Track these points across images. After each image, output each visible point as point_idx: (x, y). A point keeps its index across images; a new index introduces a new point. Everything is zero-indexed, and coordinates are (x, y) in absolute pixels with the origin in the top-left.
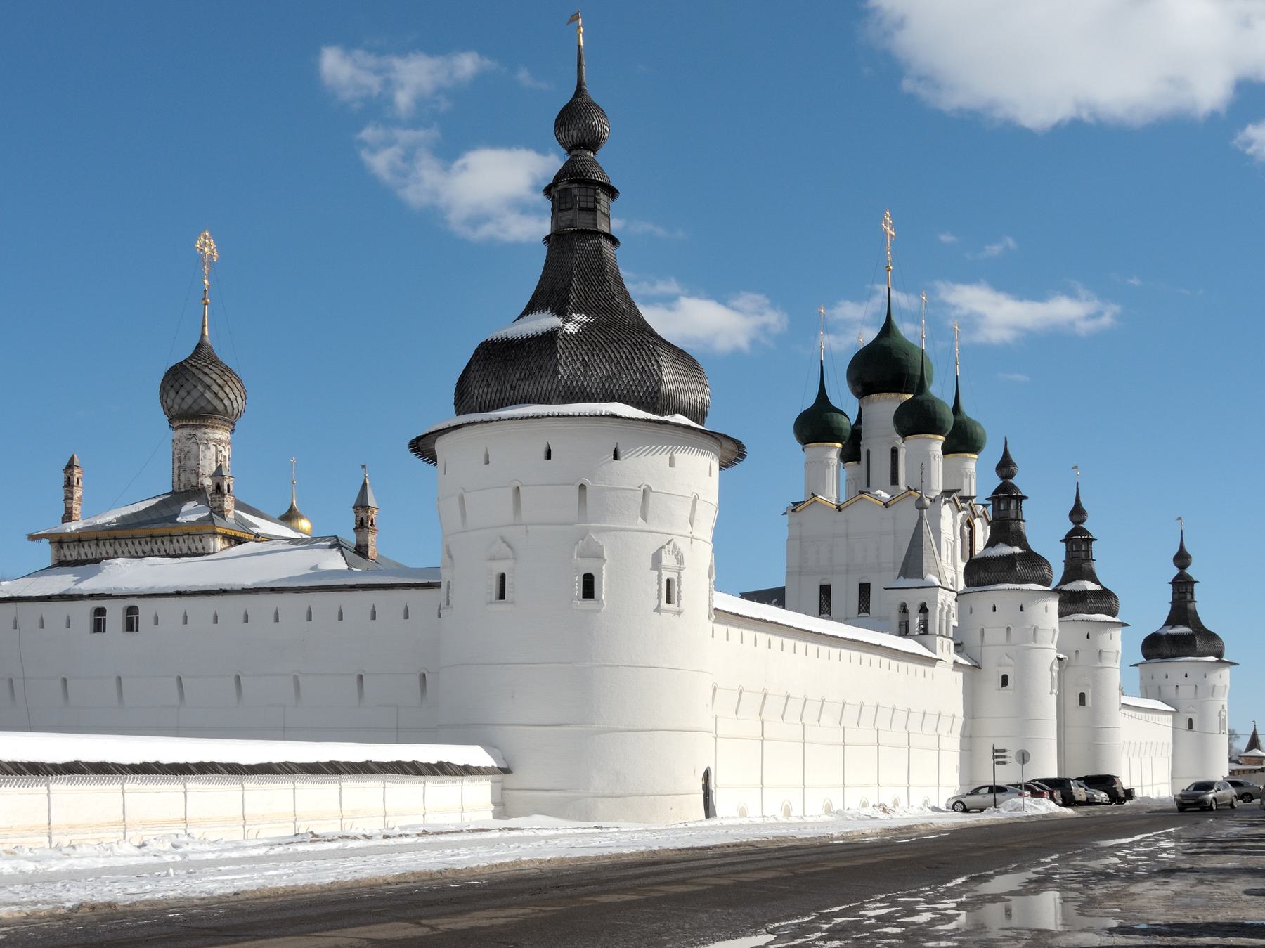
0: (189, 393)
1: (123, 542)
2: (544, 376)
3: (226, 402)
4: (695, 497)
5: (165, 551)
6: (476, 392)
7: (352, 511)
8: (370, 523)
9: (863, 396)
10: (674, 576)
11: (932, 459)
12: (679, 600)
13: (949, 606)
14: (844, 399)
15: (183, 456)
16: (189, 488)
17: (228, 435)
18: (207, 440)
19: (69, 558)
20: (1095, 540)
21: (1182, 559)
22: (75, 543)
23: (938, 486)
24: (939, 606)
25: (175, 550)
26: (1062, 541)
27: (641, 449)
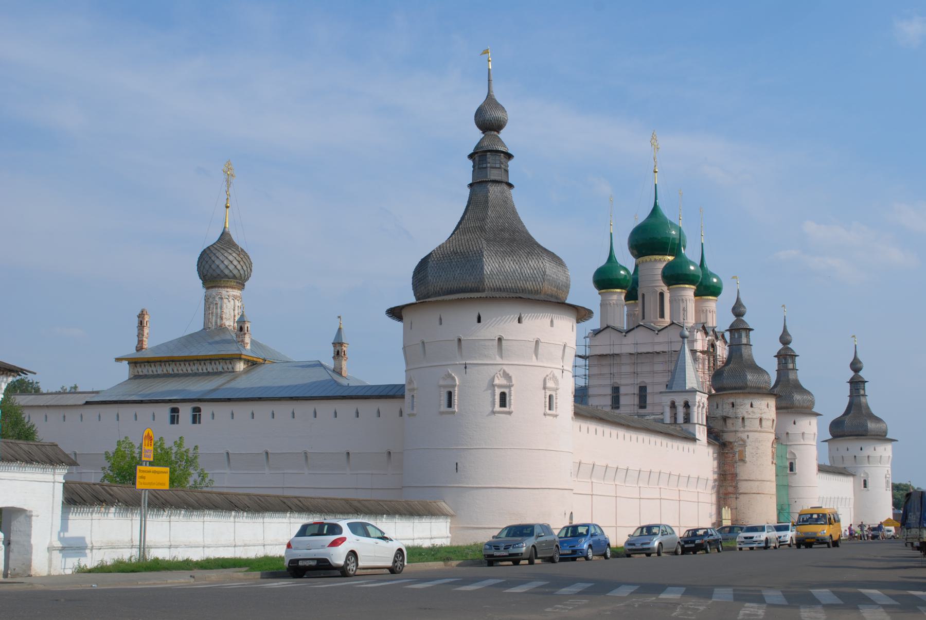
1: (178, 363)
5: (207, 369)
6: (432, 280)
7: (332, 346)
8: (343, 353)
9: (640, 257)
12: (556, 408)
13: (703, 404)
14: (627, 261)
18: (229, 296)
19: (141, 373)
20: (798, 356)
21: (856, 366)
23: (691, 320)
24: (697, 404)
25: (213, 369)
26: (775, 356)
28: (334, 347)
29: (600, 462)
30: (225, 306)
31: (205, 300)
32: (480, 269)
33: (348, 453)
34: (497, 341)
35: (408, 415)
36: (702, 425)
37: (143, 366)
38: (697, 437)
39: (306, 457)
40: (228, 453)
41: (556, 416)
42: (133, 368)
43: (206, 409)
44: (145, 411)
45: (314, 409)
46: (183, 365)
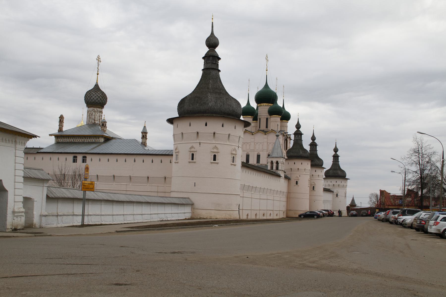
0: (93, 98)
1: (76, 138)
2: (205, 105)
5: (88, 141)
6: (187, 108)
14: (254, 105)
15: (90, 115)
16: (92, 124)
18: (97, 111)
19: (60, 141)
20: (318, 145)
21: (336, 150)
22: (62, 137)
25: (91, 141)
26: (309, 145)
30: (96, 115)
31: (87, 112)
32: (207, 104)
33: (148, 177)
34: (213, 134)
35: (175, 162)
37: (61, 138)
38: (281, 175)
39: (131, 178)
40: (97, 176)
42: (57, 139)
43: (89, 158)
44: (62, 158)
45: (152, 159)
46: (78, 138)
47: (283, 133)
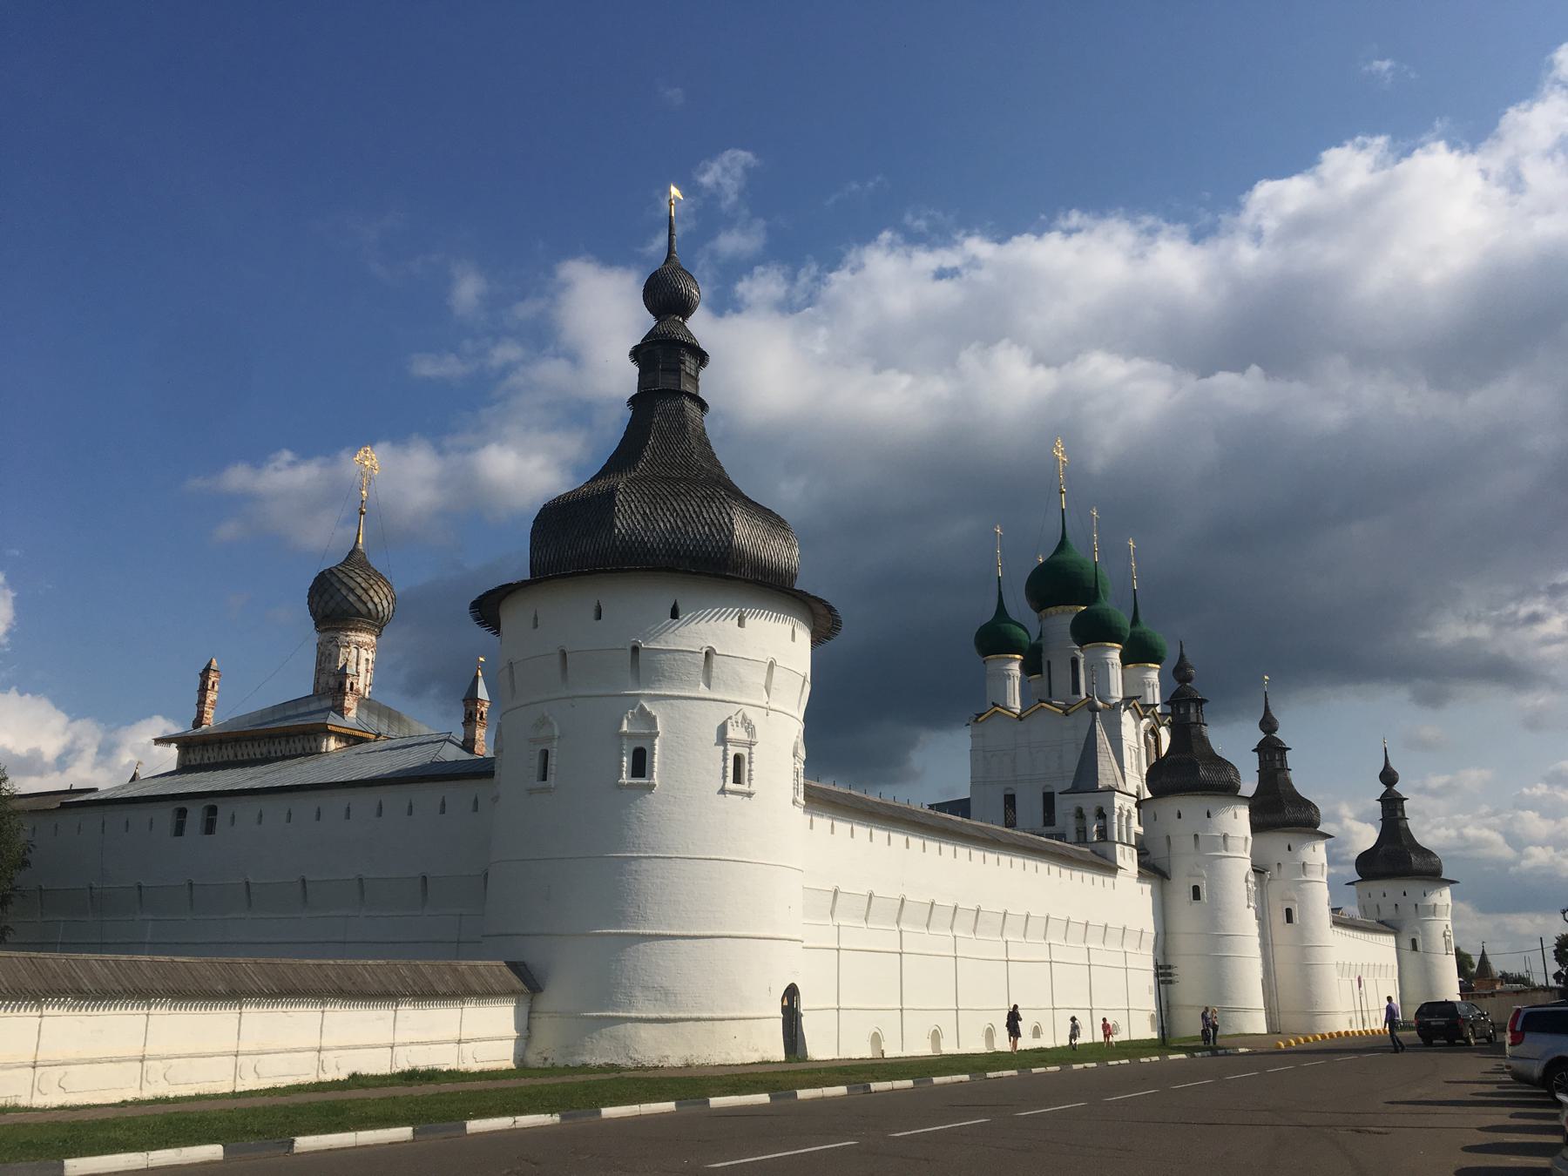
0: (332, 597)
3: (370, 605)
4: (771, 662)
7: (462, 704)
8: (478, 716)
10: (744, 751)
11: (1110, 666)
12: (750, 780)
13: (1128, 811)
17: (374, 638)
18: (348, 643)
19: (193, 763)
20: (1289, 749)
21: (1388, 776)
23: (1117, 693)
24: (1117, 810)
26: (1254, 751)
27: (703, 613)
28: (465, 705)
29: (1038, 913)
36: (1128, 844)
38: (1119, 864)
40: (247, 883)
41: (749, 795)
43: (225, 809)
47: (1134, 705)
